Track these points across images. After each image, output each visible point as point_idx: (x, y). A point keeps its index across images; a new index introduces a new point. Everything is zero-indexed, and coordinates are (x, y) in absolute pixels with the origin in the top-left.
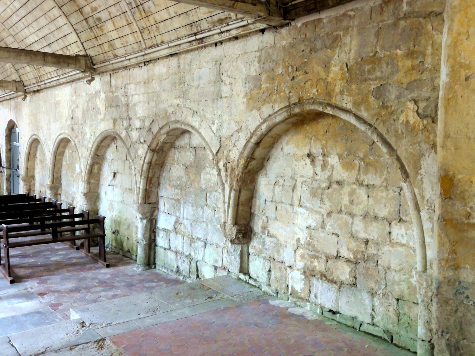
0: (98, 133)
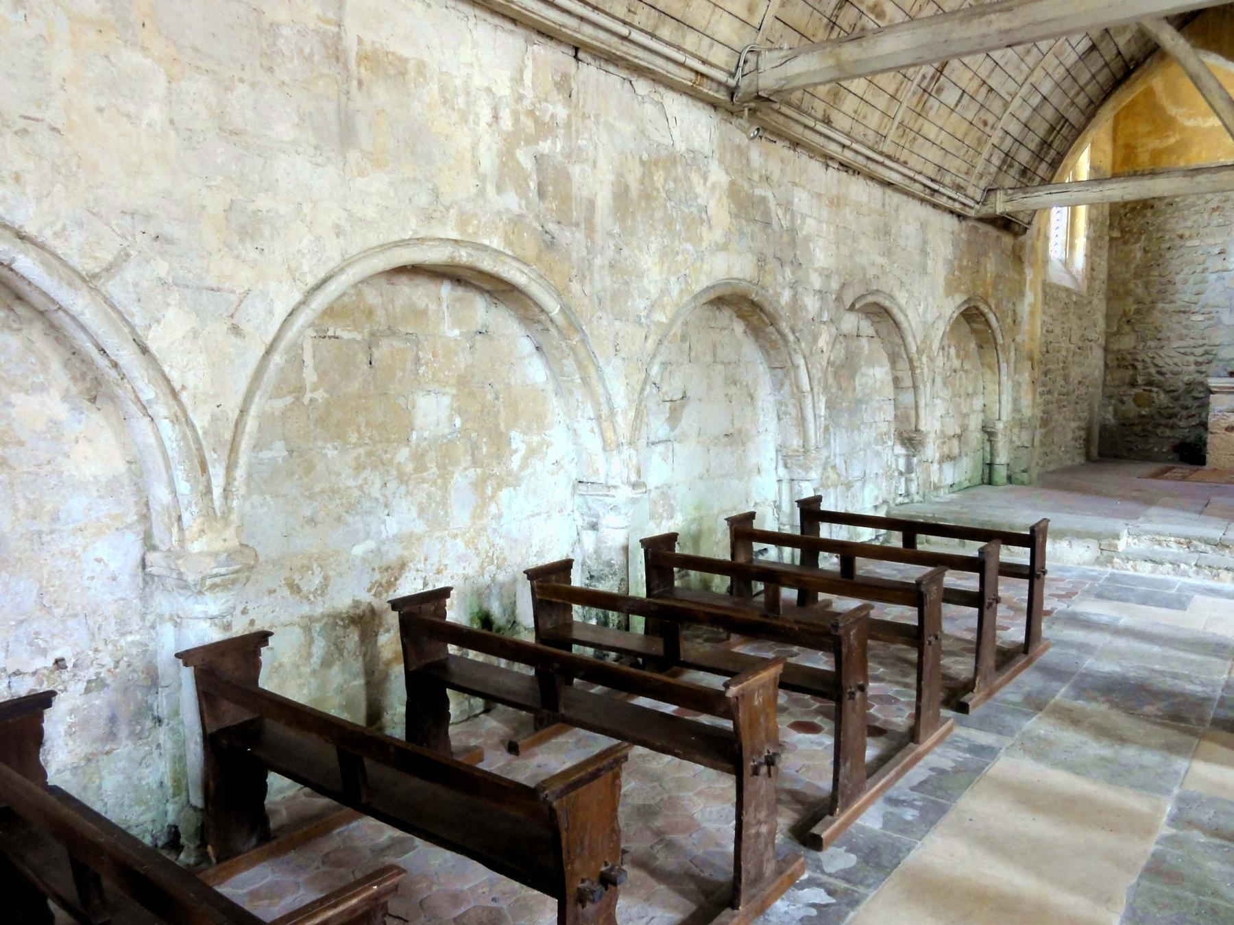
0: (705, 282)
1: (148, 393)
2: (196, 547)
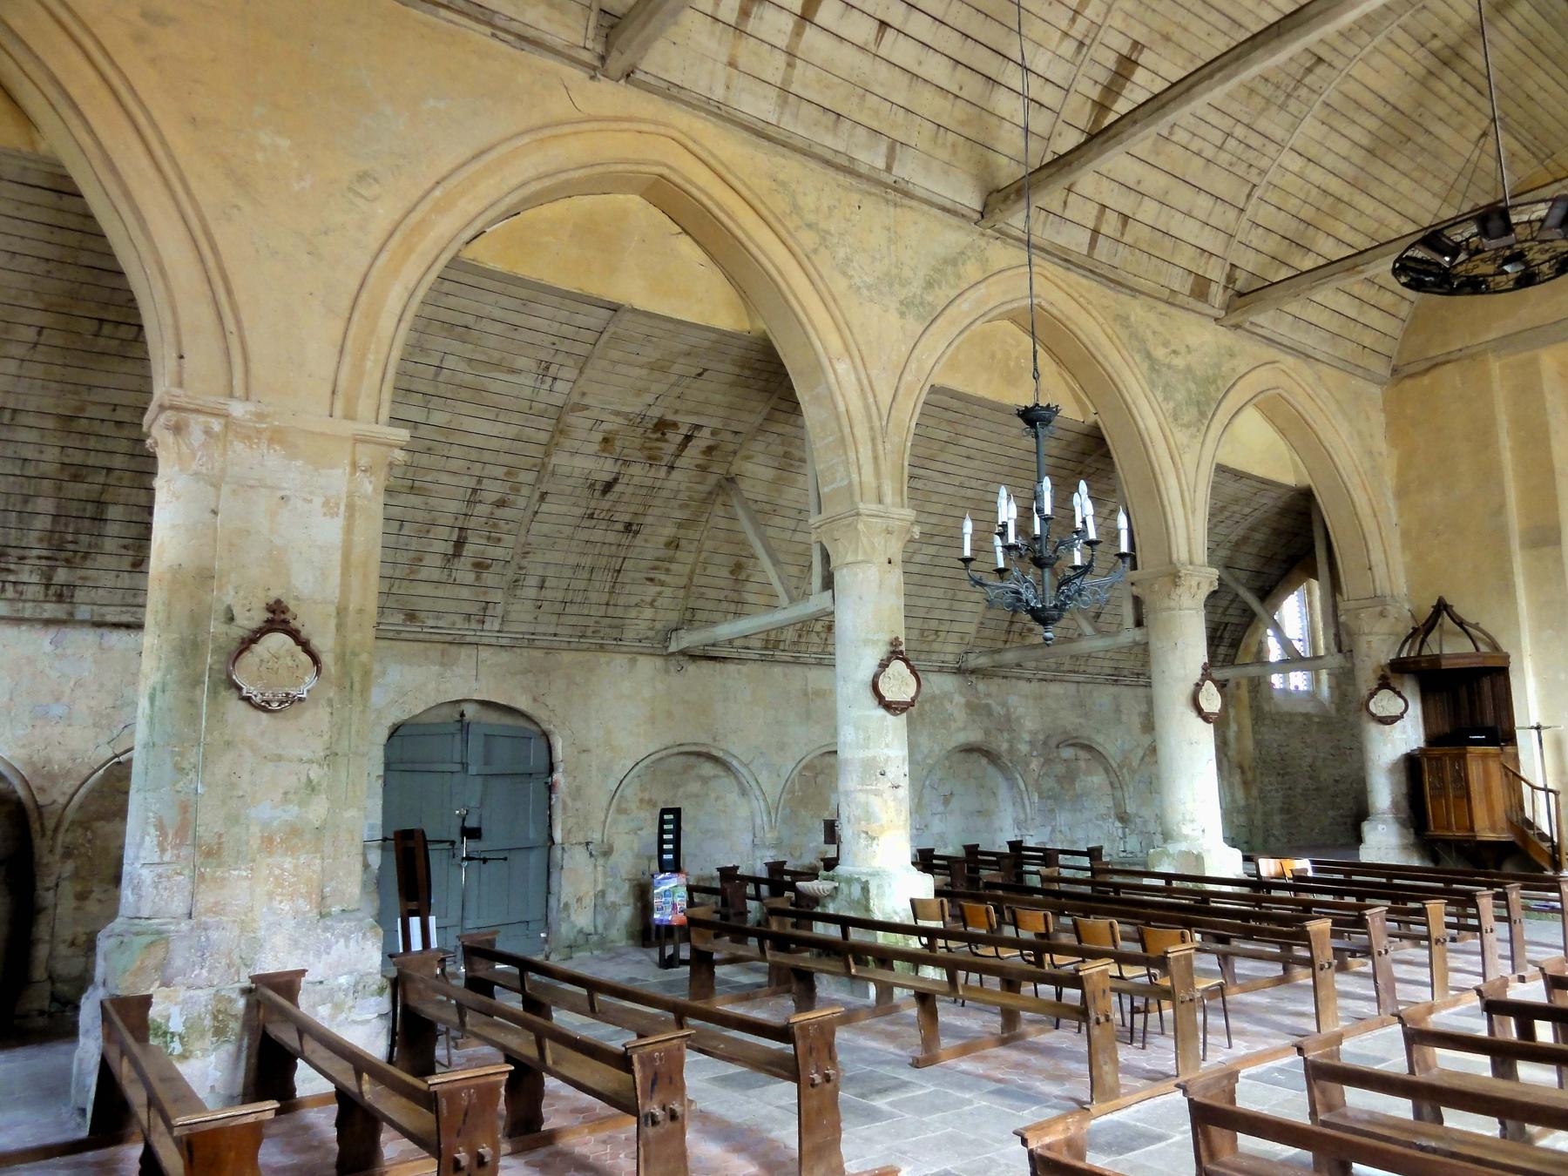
1: (758, 793)
2: (768, 836)
